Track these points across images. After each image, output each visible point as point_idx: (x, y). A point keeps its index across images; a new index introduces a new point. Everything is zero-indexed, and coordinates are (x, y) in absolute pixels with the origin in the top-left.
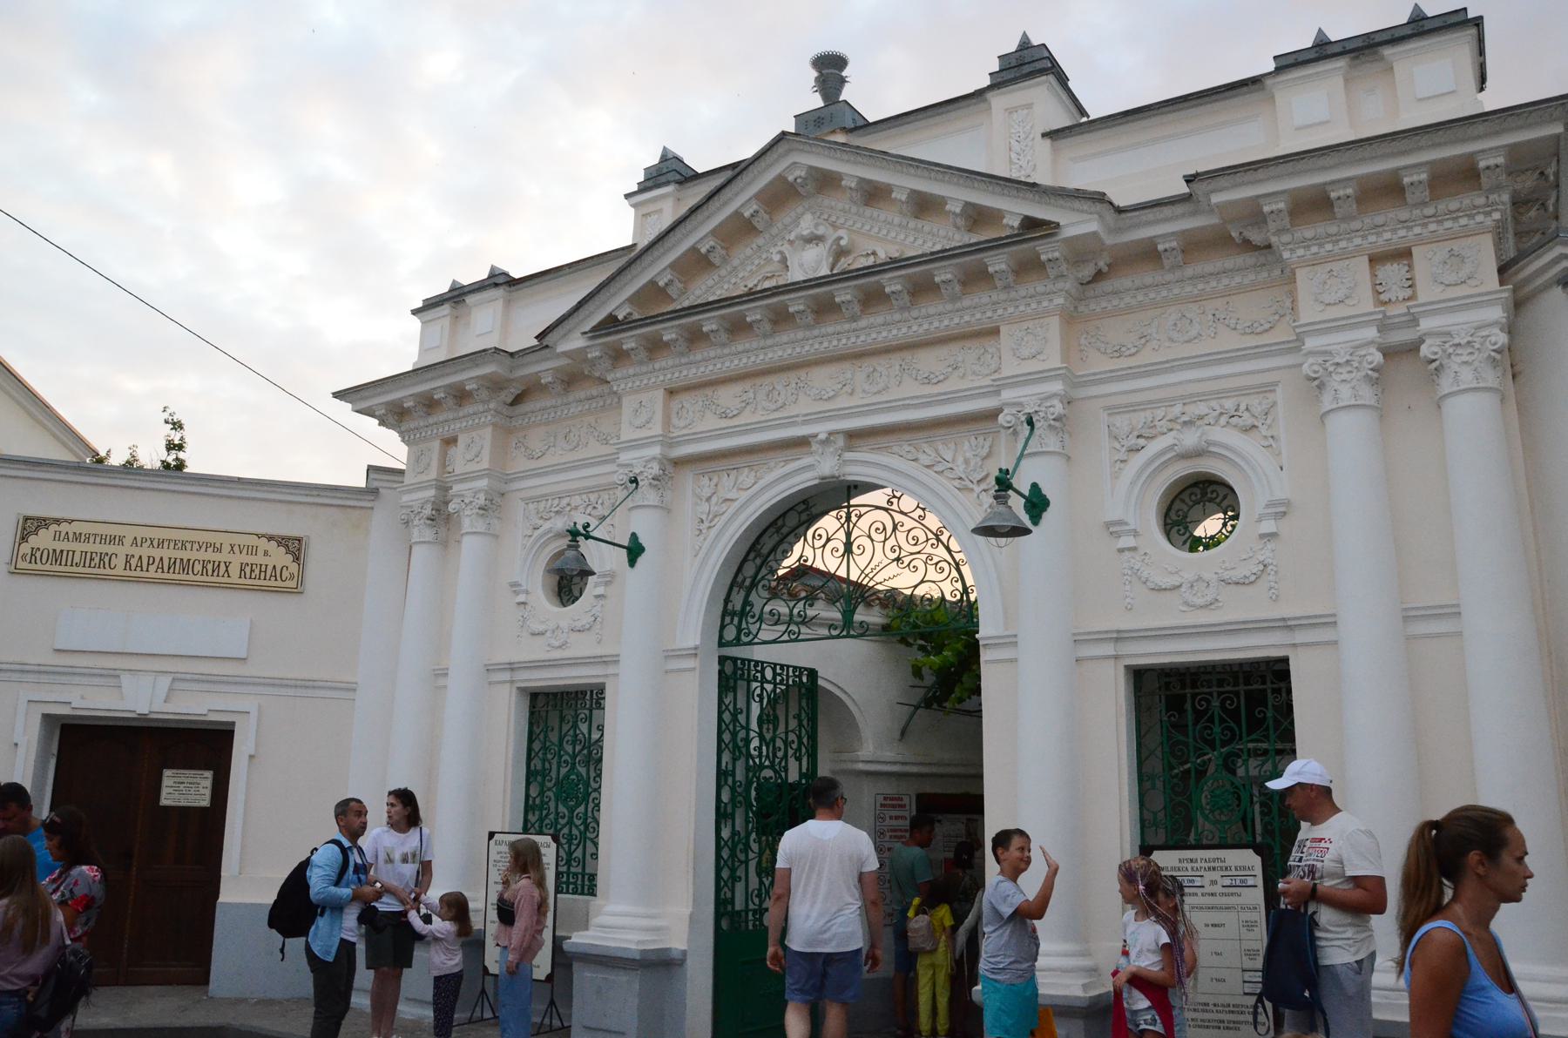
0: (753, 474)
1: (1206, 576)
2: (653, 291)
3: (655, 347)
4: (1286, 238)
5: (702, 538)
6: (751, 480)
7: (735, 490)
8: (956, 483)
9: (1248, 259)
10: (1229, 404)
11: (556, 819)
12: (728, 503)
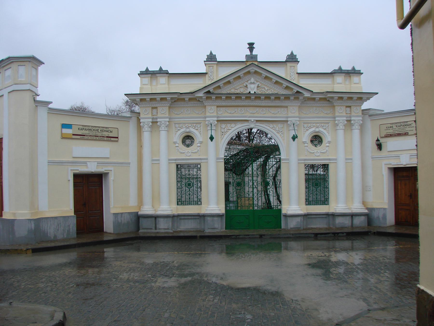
1: (318, 151)
2: (219, 87)
3: (217, 98)
4: (335, 102)
5: (223, 136)
7: (230, 127)
8: (276, 132)
9: (328, 102)
10: (322, 125)
12: (228, 130)
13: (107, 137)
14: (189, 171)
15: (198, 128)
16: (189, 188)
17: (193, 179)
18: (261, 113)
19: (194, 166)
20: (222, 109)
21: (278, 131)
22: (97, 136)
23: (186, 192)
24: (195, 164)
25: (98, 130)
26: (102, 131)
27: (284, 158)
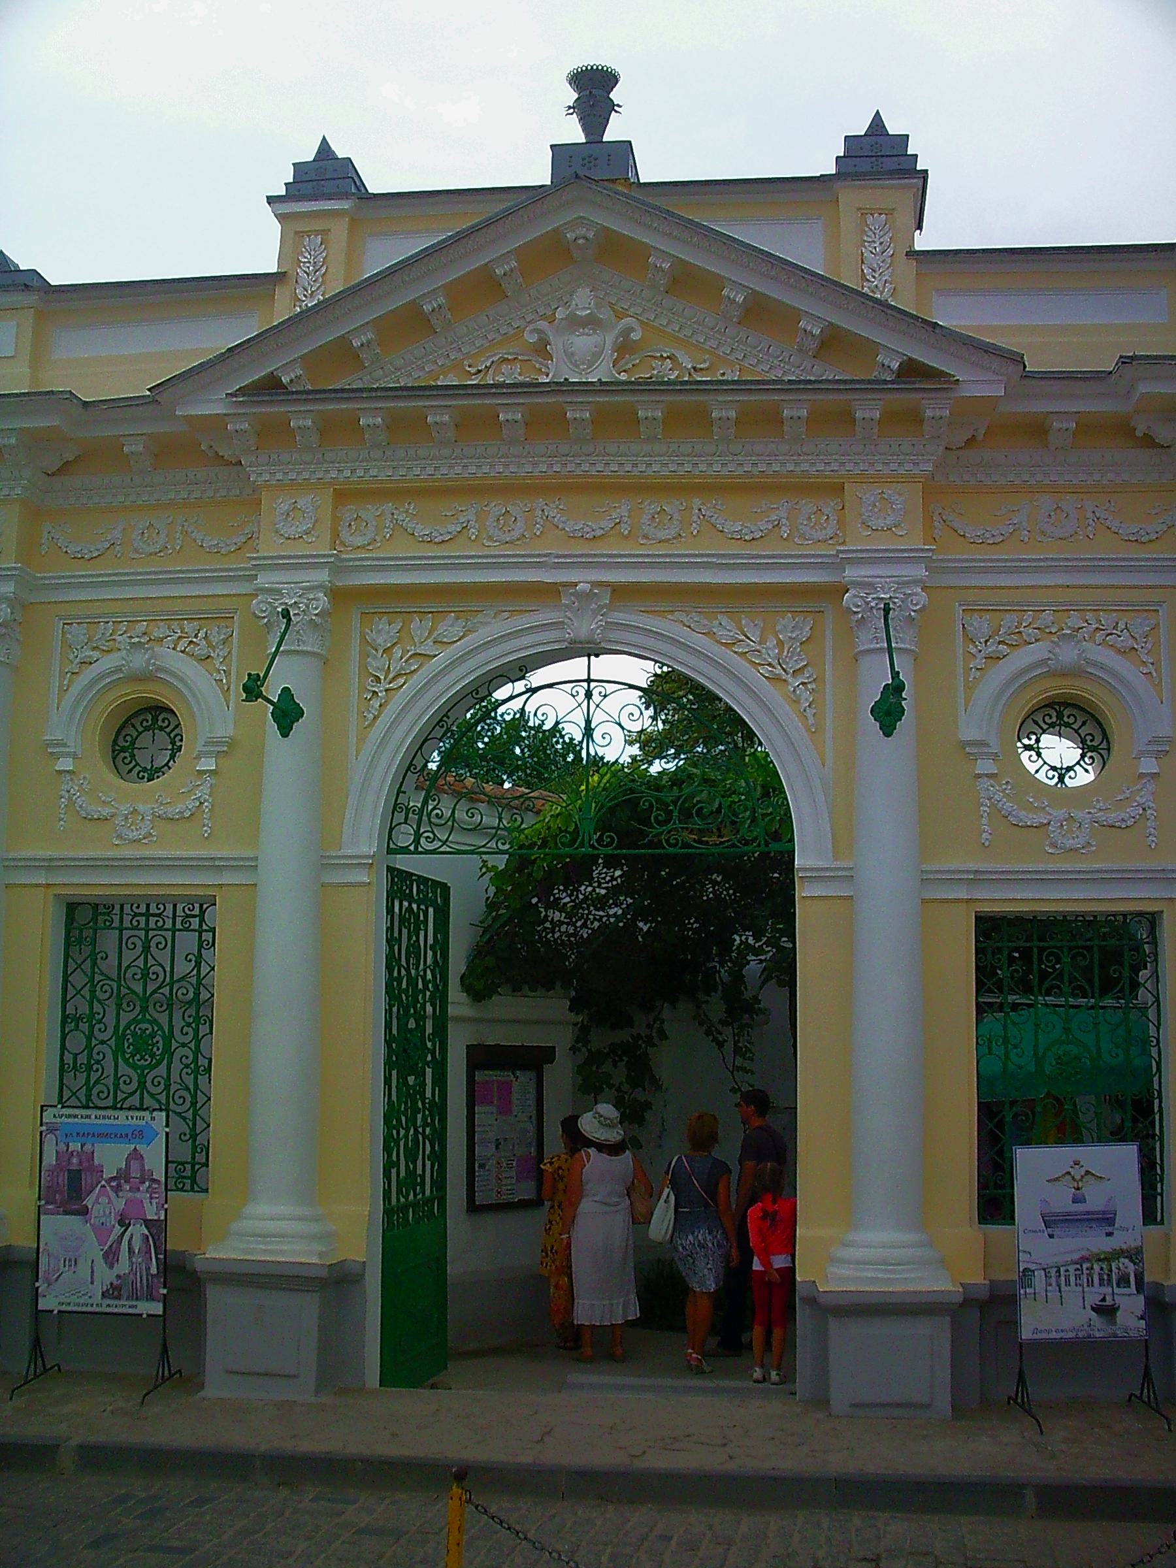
0: (462, 622)
6: (457, 630)
11: (117, 1086)
12: (422, 659)
14: (146, 949)
15: (210, 645)
16: (143, 1068)
17: (170, 1006)
18: (646, 537)
19: (179, 912)
20: (370, 512)
21: (775, 663)
23: (120, 1096)
24: (190, 900)
27: (811, 863)
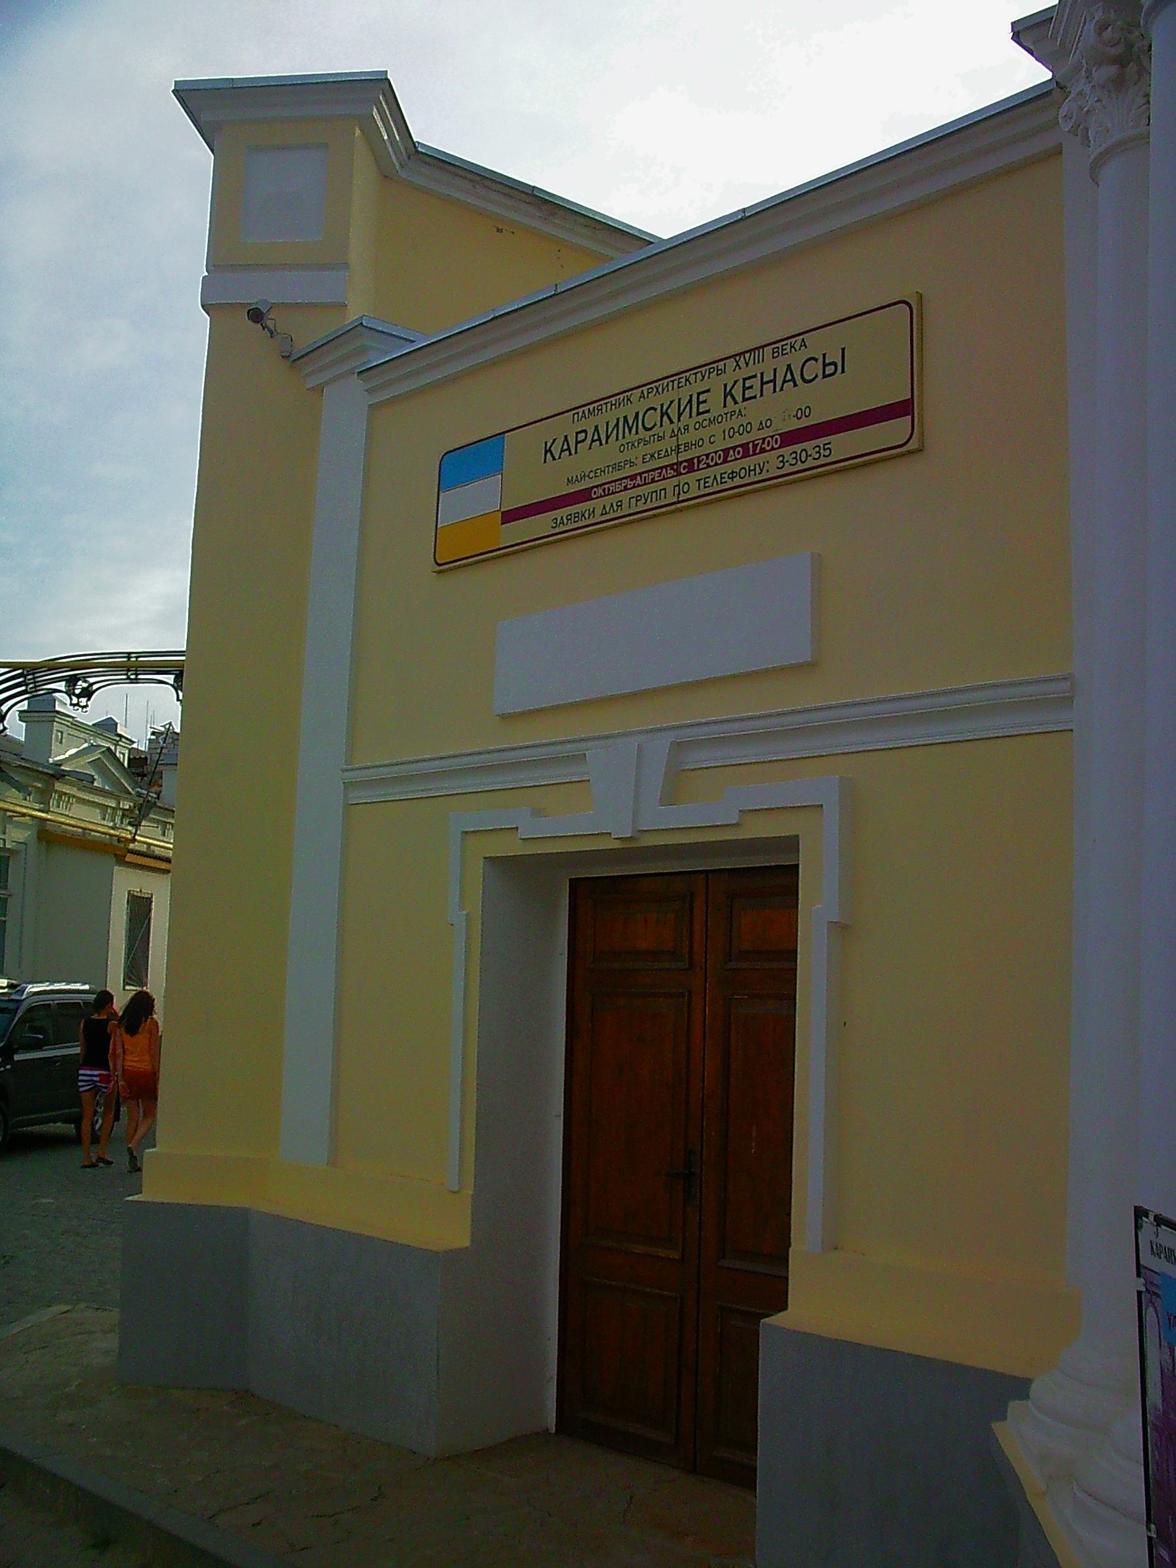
13: (789, 438)
22: (691, 466)
25: (698, 402)
26: (739, 399)
